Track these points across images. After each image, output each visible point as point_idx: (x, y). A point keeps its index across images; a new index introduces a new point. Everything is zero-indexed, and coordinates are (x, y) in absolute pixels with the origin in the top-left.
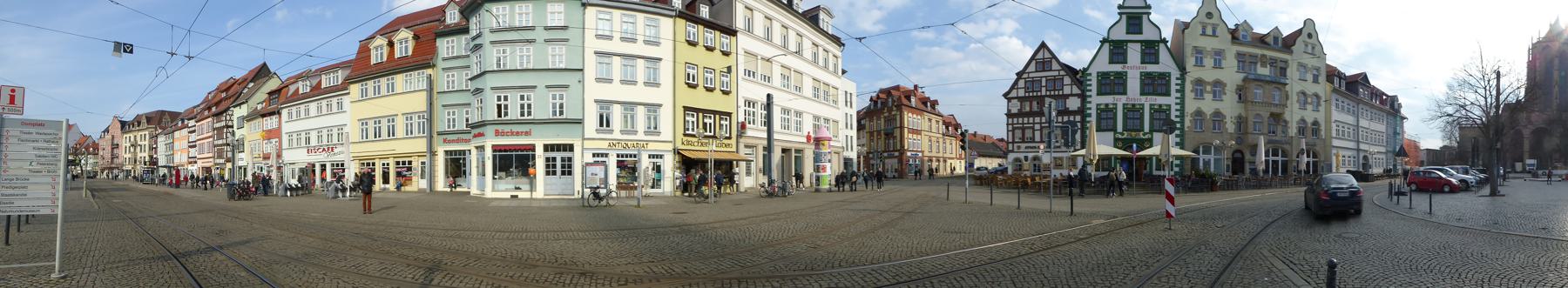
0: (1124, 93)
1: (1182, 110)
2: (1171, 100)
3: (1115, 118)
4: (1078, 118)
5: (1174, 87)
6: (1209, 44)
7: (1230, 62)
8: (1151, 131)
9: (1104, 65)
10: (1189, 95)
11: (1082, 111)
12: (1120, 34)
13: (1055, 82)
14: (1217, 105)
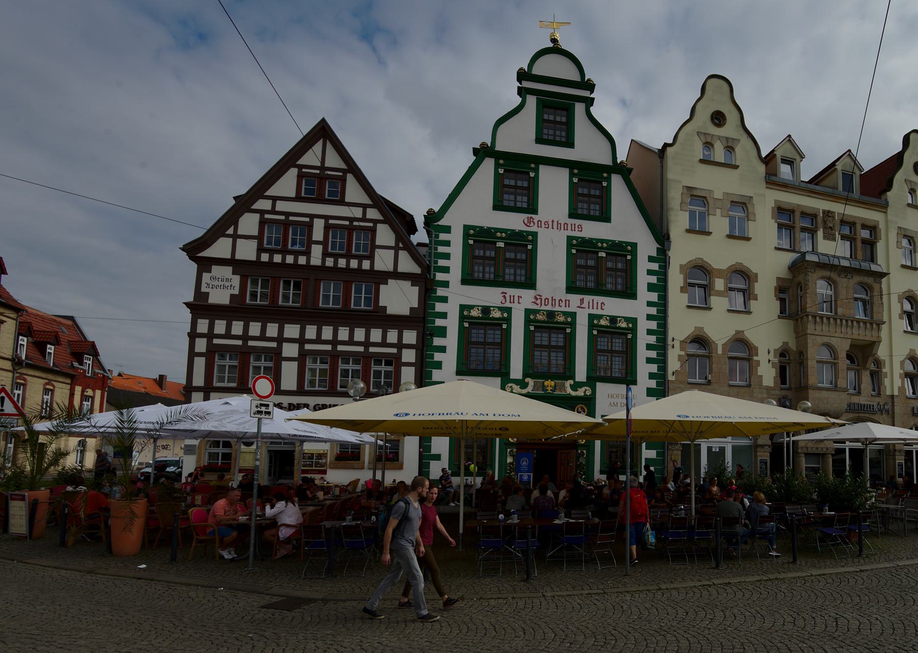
0: (530, 283)
1: (661, 332)
2: (636, 308)
3: (504, 345)
4: (410, 337)
5: (643, 280)
6: (718, 183)
7: (764, 227)
8: (592, 380)
9: (478, 209)
10: (677, 299)
11: (422, 320)
12: (520, 138)
13: (351, 237)
14: (740, 323)
